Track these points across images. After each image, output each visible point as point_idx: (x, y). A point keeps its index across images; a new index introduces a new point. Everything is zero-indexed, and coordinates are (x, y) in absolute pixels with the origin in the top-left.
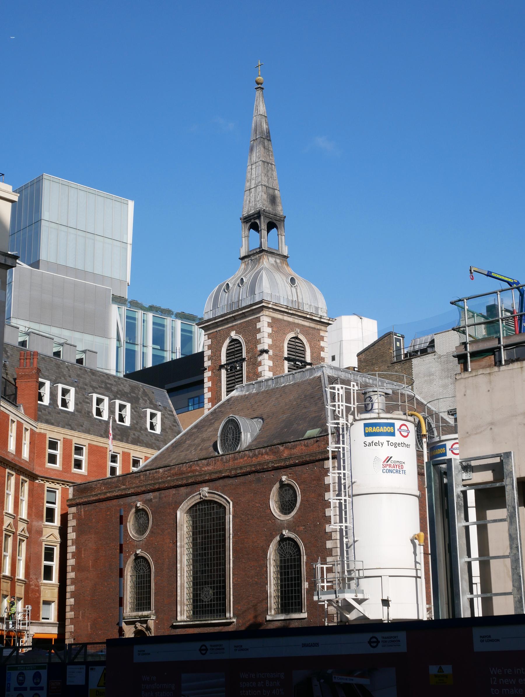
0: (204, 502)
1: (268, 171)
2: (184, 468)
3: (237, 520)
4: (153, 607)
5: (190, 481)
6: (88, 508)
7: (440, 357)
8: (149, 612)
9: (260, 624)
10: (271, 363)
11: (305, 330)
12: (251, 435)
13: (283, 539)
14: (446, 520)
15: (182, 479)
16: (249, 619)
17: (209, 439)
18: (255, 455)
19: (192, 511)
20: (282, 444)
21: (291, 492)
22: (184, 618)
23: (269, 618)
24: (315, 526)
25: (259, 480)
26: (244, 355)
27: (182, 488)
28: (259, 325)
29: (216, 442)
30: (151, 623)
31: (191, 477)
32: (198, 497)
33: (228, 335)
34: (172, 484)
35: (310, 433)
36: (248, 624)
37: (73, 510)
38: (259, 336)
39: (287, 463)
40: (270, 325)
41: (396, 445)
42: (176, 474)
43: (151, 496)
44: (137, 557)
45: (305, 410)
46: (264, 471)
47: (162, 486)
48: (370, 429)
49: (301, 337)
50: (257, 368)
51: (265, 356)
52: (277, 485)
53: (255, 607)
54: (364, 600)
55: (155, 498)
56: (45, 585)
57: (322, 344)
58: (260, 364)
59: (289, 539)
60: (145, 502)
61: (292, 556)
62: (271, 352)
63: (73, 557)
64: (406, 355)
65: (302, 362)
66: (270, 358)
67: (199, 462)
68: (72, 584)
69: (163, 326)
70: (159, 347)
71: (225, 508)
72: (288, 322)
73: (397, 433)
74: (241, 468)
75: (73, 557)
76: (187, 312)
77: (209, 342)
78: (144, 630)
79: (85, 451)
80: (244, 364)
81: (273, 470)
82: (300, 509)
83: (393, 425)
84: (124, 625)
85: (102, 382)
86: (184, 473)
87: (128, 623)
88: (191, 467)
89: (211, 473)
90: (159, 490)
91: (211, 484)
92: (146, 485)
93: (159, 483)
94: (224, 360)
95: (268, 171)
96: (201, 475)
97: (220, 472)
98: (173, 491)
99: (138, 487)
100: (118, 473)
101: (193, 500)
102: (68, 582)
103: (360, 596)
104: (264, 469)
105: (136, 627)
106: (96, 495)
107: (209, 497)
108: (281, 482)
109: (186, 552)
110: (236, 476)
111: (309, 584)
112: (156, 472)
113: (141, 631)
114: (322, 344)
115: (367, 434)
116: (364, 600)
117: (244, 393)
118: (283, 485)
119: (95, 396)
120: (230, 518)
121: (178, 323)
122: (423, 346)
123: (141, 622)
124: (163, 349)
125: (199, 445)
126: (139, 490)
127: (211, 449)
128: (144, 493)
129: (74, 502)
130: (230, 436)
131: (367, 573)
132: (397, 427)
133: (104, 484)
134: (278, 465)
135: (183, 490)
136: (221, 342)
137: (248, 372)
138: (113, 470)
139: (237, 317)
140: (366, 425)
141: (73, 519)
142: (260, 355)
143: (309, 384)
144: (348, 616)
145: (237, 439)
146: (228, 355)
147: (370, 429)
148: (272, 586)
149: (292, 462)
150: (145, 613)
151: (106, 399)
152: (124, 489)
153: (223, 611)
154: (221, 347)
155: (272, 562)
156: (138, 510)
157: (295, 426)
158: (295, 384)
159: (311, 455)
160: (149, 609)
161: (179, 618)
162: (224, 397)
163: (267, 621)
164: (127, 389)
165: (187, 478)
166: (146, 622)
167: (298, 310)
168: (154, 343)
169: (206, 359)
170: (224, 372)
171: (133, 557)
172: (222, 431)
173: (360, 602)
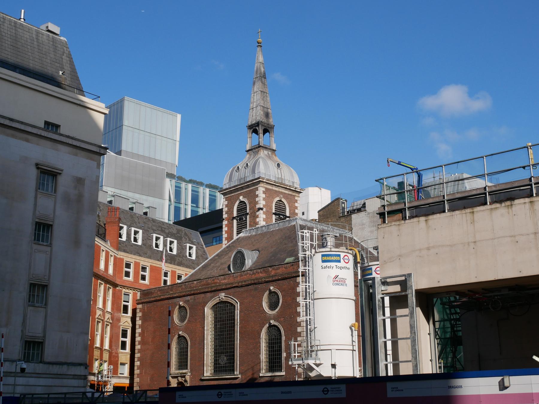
0: (221, 302)
1: (264, 97)
2: (210, 281)
3: (242, 314)
4: (189, 367)
6: (149, 305)
7: (369, 214)
8: (186, 371)
9: (256, 379)
10: (264, 216)
11: (286, 196)
12: (252, 261)
13: (271, 326)
14: (371, 316)
15: (208, 288)
16: (249, 375)
17: (225, 263)
18: (254, 273)
19: (215, 308)
20: (270, 267)
21: (276, 296)
22: (209, 374)
23: (261, 375)
24: (291, 318)
25: (256, 289)
26: (248, 211)
27: (208, 294)
28: (257, 193)
29: (230, 265)
30: (188, 378)
31: (214, 287)
32: (218, 299)
33: (238, 198)
34: (202, 291)
35: (288, 260)
36: (248, 379)
37: (140, 306)
38: (257, 199)
39: (274, 279)
40: (264, 192)
41: (341, 268)
42: (204, 285)
43: (188, 298)
44: (180, 336)
45: (285, 246)
47: (196, 292)
48: (325, 258)
49: (283, 200)
50: (256, 219)
51: (261, 211)
52: (267, 292)
53: (253, 367)
54: (320, 364)
55: (191, 299)
56: (122, 353)
57: (296, 205)
58: (257, 217)
59: (274, 326)
60: (185, 302)
62: (264, 210)
63: (139, 336)
64: (348, 212)
65: (283, 215)
66: (264, 213)
67: (219, 277)
68: (139, 352)
69: (198, 192)
70: (195, 205)
71: (235, 306)
72: (276, 191)
73: (342, 260)
74: (245, 281)
75: (139, 336)
76: (213, 184)
77: (226, 203)
78: (183, 381)
79: (148, 269)
80: (248, 217)
82: (281, 307)
83: (339, 256)
84: (170, 378)
85: (159, 227)
87: (173, 377)
88: (214, 280)
89: (226, 284)
90: (194, 294)
91: (226, 291)
92: (186, 291)
93: (194, 290)
94: (235, 214)
95: (264, 97)
96: (220, 286)
97: (232, 283)
98: (203, 295)
99: (181, 292)
100: (168, 283)
101: (215, 301)
102: (136, 351)
103: (318, 362)
105: (178, 380)
106: (154, 297)
107: (225, 299)
108: (270, 290)
109: (210, 333)
110: (242, 286)
113: (181, 382)
114: (296, 205)
115: (323, 261)
116: (320, 364)
117: (247, 235)
118: (271, 292)
119: (155, 236)
120: (237, 312)
121: (207, 191)
122: (358, 207)
123: (182, 377)
124: (197, 207)
125: (219, 267)
126: (181, 294)
127: (227, 269)
128: (184, 296)
129: (140, 301)
130: (239, 261)
131: (322, 348)
132: (342, 256)
133: (160, 290)
135: (209, 295)
137: (250, 222)
138: (165, 281)
140: (323, 256)
141: (140, 312)
142: (258, 211)
143: (288, 229)
144: (310, 374)
145: (243, 263)
146: (238, 211)
147: (325, 258)
148: (264, 355)
149: (277, 278)
150: (184, 371)
151: (162, 238)
152: (172, 294)
153: (233, 370)
154: (234, 206)
155: (264, 340)
156: (180, 307)
157: (279, 255)
158: (279, 229)
159: (288, 274)
160: (187, 369)
161: (205, 375)
162: (235, 237)
163: (260, 377)
164: (175, 231)
166: (184, 377)
167: (281, 183)
168: (192, 203)
169: (224, 213)
170: (235, 221)
171: (177, 336)
172: (234, 258)
173: (318, 365)
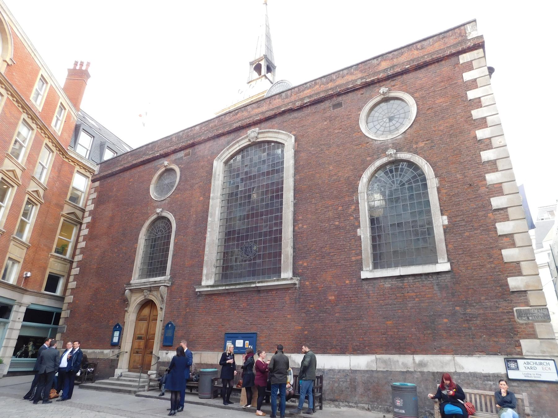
5: (235, 126)
22: (211, 282)
32: (247, 140)
37: (97, 184)
39: (390, 73)
43: (182, 154)
46: (348, 93)
55: (186, 155)
61: (404, 184)
74: (310, 96)
75: (87, 227)
81: (362, 88)
89: (263, 113)
91: (263, 125)
97: (278, 108)
98: (209, 144)
104: (348, 89)
111: (449, 218)
112: (191, 131)
128: (175, 152)
134: (372, 79)
135: (223, 140)
141: (95, 192)
149: (398, 70)
153: (277, 271)
160: (164, 274)
161: (204, 283)
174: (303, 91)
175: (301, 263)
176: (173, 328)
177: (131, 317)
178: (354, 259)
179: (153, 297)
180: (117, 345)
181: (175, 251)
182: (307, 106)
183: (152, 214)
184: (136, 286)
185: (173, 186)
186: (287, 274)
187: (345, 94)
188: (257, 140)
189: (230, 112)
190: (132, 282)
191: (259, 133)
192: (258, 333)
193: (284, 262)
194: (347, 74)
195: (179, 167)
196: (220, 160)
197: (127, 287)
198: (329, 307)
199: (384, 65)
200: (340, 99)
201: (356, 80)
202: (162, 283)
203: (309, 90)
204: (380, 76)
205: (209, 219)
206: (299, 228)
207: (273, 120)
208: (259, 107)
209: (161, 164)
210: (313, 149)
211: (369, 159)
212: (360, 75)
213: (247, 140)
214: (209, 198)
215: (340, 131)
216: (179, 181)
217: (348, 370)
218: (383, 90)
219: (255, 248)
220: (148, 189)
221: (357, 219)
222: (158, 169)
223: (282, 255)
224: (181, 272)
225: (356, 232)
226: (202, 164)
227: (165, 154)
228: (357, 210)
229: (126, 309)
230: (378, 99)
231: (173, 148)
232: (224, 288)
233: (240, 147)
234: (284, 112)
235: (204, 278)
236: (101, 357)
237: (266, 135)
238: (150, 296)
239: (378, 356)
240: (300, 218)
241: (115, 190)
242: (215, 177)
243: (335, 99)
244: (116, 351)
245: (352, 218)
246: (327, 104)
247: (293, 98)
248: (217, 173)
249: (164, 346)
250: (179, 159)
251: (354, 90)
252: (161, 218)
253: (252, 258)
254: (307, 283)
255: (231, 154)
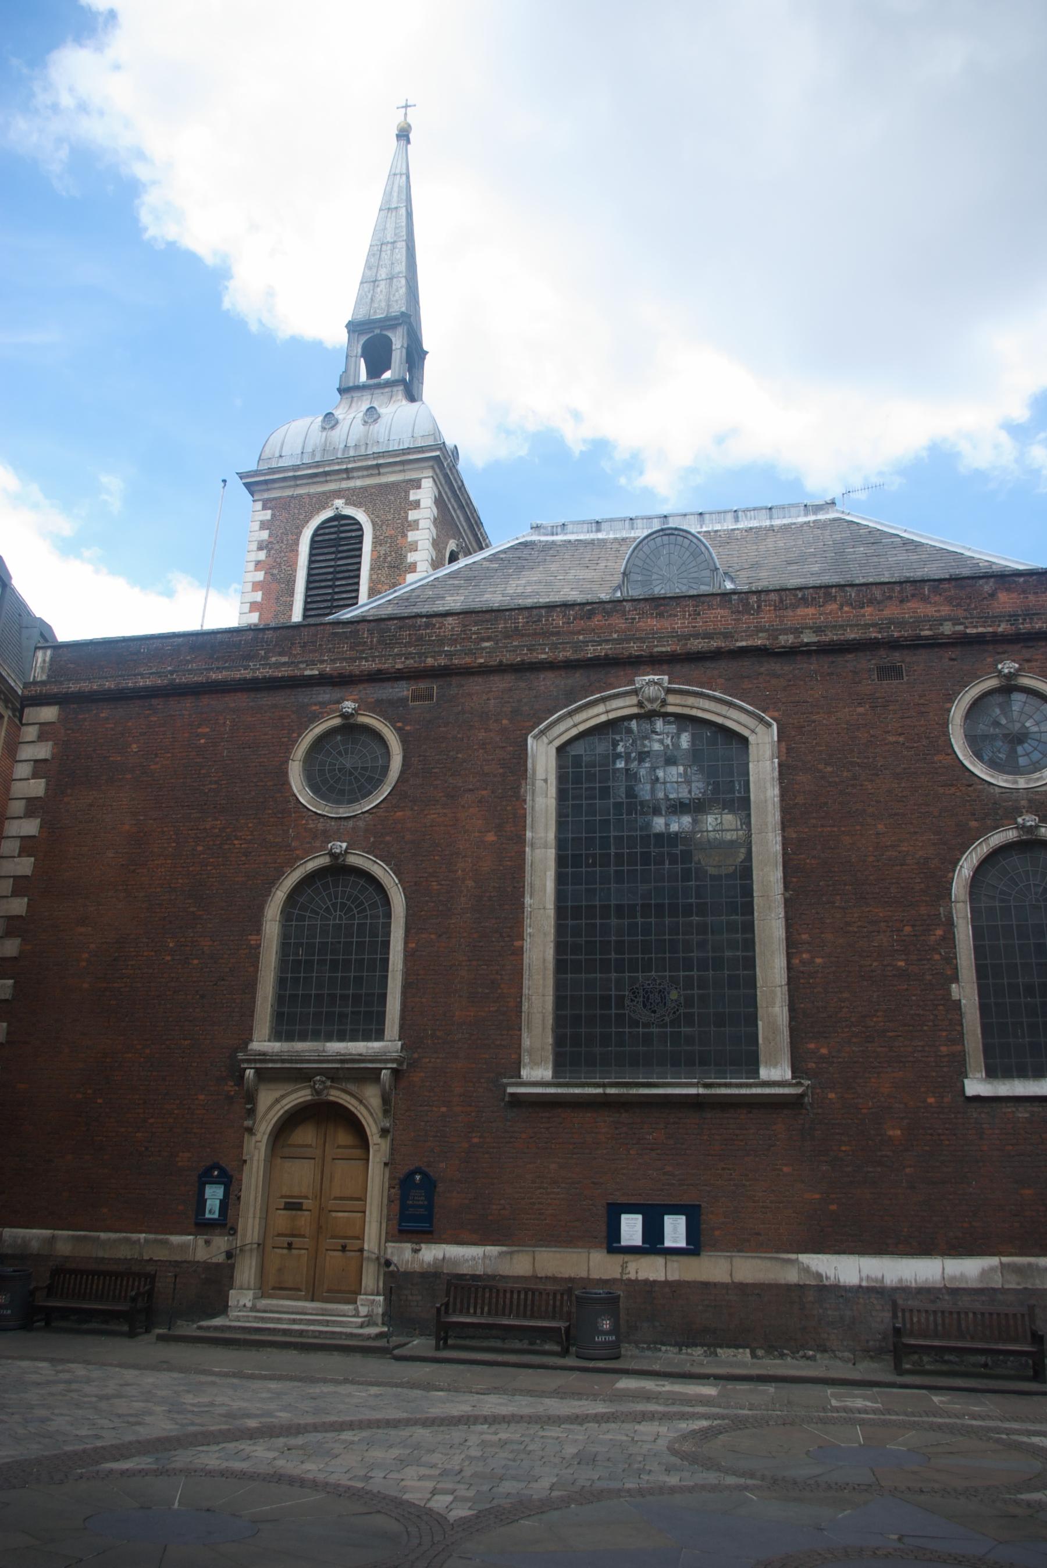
5: (591, 651)
8: (376, 1045)
18: (871, 602)
32: (634, 700)
34: (508, 658)
39: (1025, 627)
43: (403, 690)
74: (818, 630)
86: (558, 633)
97: (727, 636)
98: (500, 683)
104: (919, 638)
112: (427, 626)
134: (981, 630)
135: (548, 682)
136: (301, 517)
139: (355, 474)
160: (379, 1036)
161: (524, 1073)
165: (577, 647)
174: (794, 607)
175: (812, 1046)
176: (429, 1184)
177: (257, 1148)
178: (944, 1049)
179: (348, 1098)
180: (226, 1223)
181: (407, 973)
182: (809, 653)
183: (307, 853)
184: (283, 1061)
185: (377, 783)
186: (776, 1072)
187: (908, 647)
188: (663, 710)
189: (566, 606)
190: (256, 1046)
191: (669, 691)
192: (704, 1205)
193: (765, 1038)
194: (913, 596)
195: (399, 730)
196: (545, 739)
197: (248, 1061)
198: (889, 1153)
199: (1006, 601)
200: (897, 656)
201: (941, 621)
202: (386, 1061)
203: (811, 611)
204: (1000, 629)
205: (528, 900)
206: (803, 962)
207: (708, 664)
208: (661, 615)
209: (323, 704)
210: (829, 769)
211: (973, 824)
212: (945, 610)
213: (634, 700)
214: (521, 840)
215: (901, 739)
216: (402, 772)
217: (940, 1289)
218: (1008, 666)
219: (674, 995)
220: (285, 774)
221: (951, 960)
222: (315, 718)
223: (760, 1023)
224: (438, 1034)
225: (949, 991)
226: (481, 735)
227: (341, 676)
228: (949, 939)
229: (248, 1123)
230: (992, 683)
231: (367, 666)
232: (600, 1091)
233: (612, 715)
234: (743, 652)
235: (526, 1059)
236: (161, 1254)
237: (691, 700)
238: (333, 1092)
239: (1005, 1259)
240: (805, 937)
241: (135, 747)
242: (533, 785)
243: (882, 652)
244: (221, 1243)
245: (937, 957)
246: (866, 663)
247: (767, 617)
248: (540, 774)
249: (401, 1231)
250: (391, 702)
251: (934, 644)
252: (338, 870)
253: (667, 1019)
254: (832, 1095)
255: (582, 728)
